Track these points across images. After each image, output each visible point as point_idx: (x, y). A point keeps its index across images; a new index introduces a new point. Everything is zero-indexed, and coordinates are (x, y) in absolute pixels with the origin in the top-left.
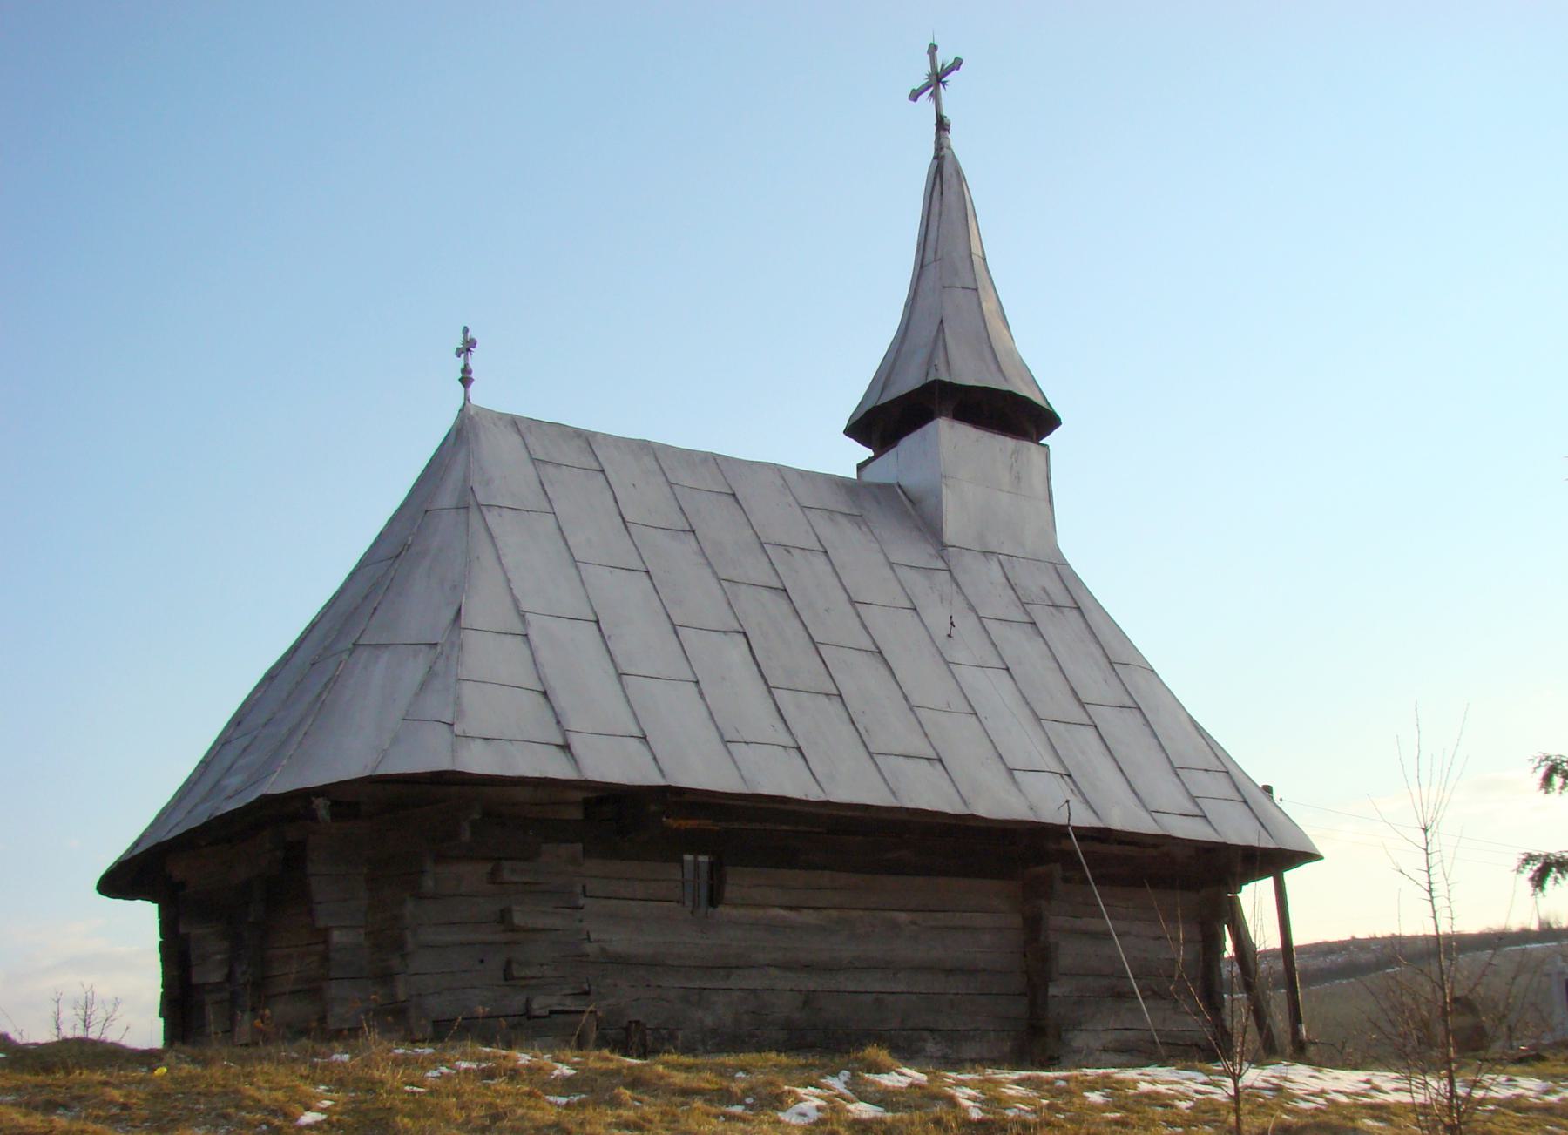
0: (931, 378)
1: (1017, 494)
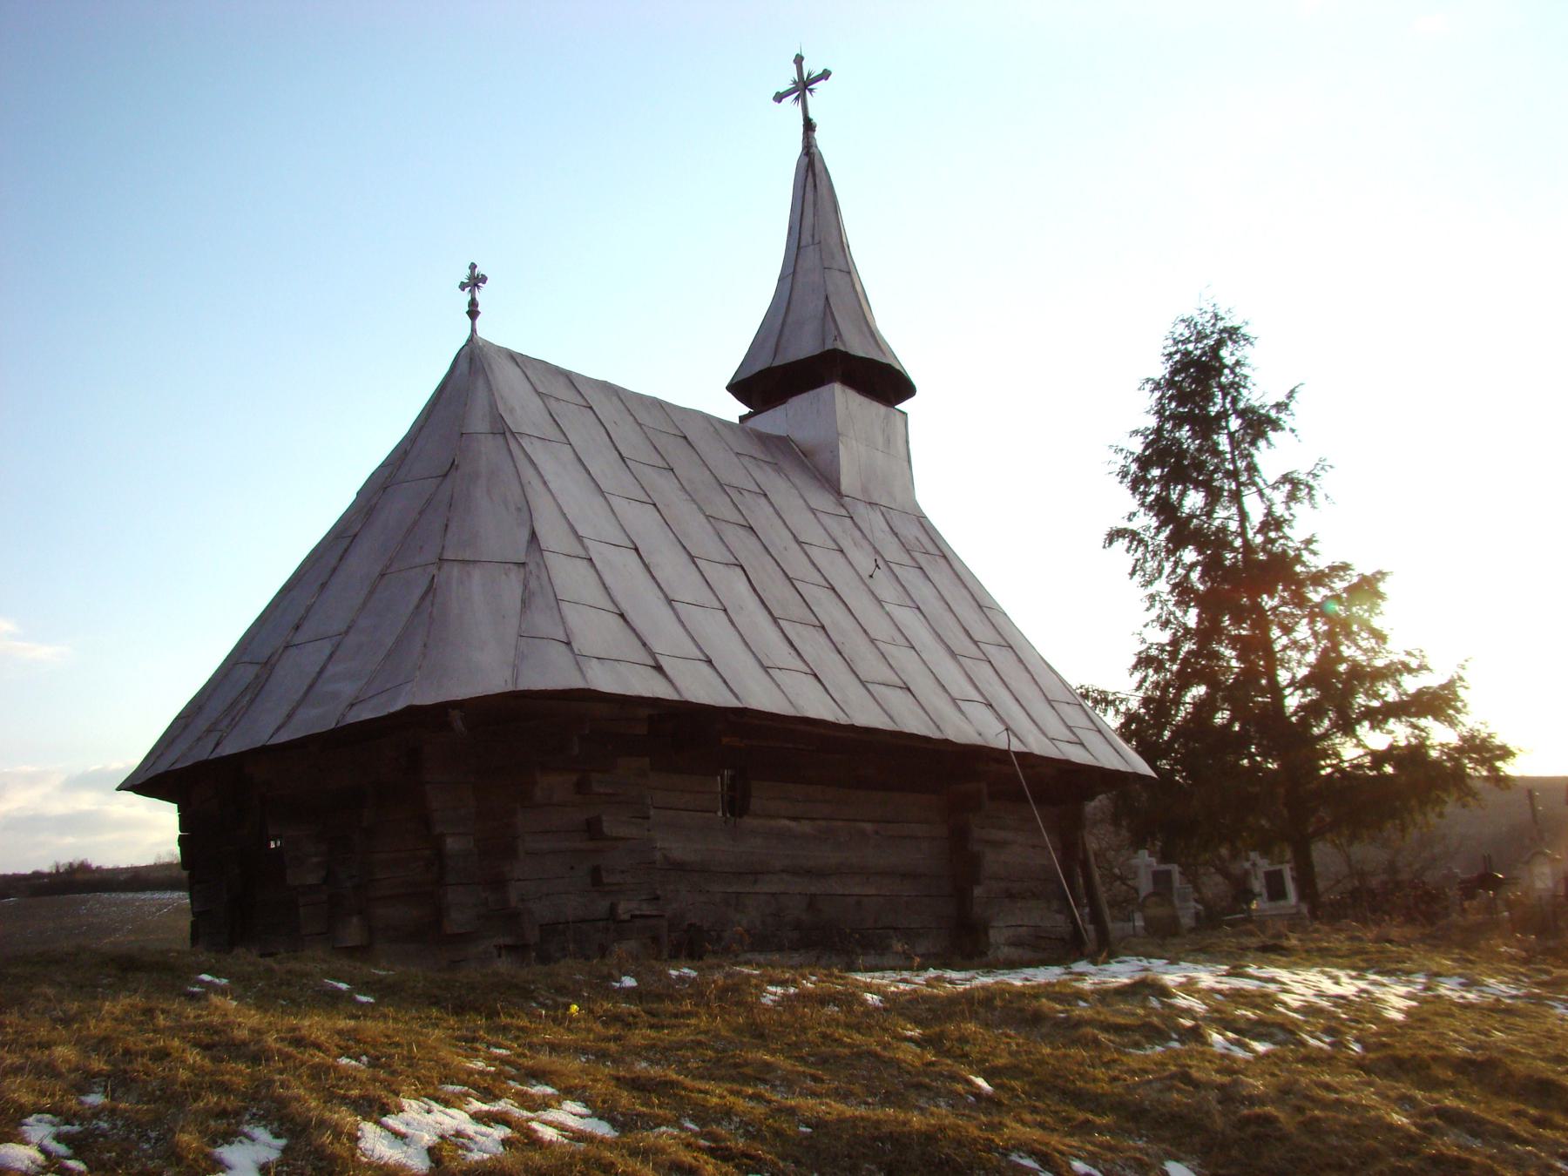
0: (829, 346)
1: (888, 454)
